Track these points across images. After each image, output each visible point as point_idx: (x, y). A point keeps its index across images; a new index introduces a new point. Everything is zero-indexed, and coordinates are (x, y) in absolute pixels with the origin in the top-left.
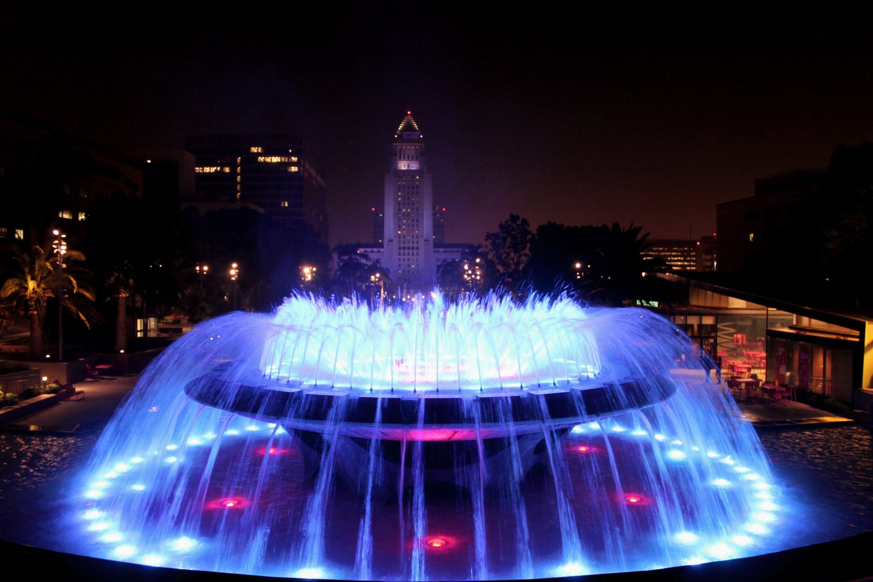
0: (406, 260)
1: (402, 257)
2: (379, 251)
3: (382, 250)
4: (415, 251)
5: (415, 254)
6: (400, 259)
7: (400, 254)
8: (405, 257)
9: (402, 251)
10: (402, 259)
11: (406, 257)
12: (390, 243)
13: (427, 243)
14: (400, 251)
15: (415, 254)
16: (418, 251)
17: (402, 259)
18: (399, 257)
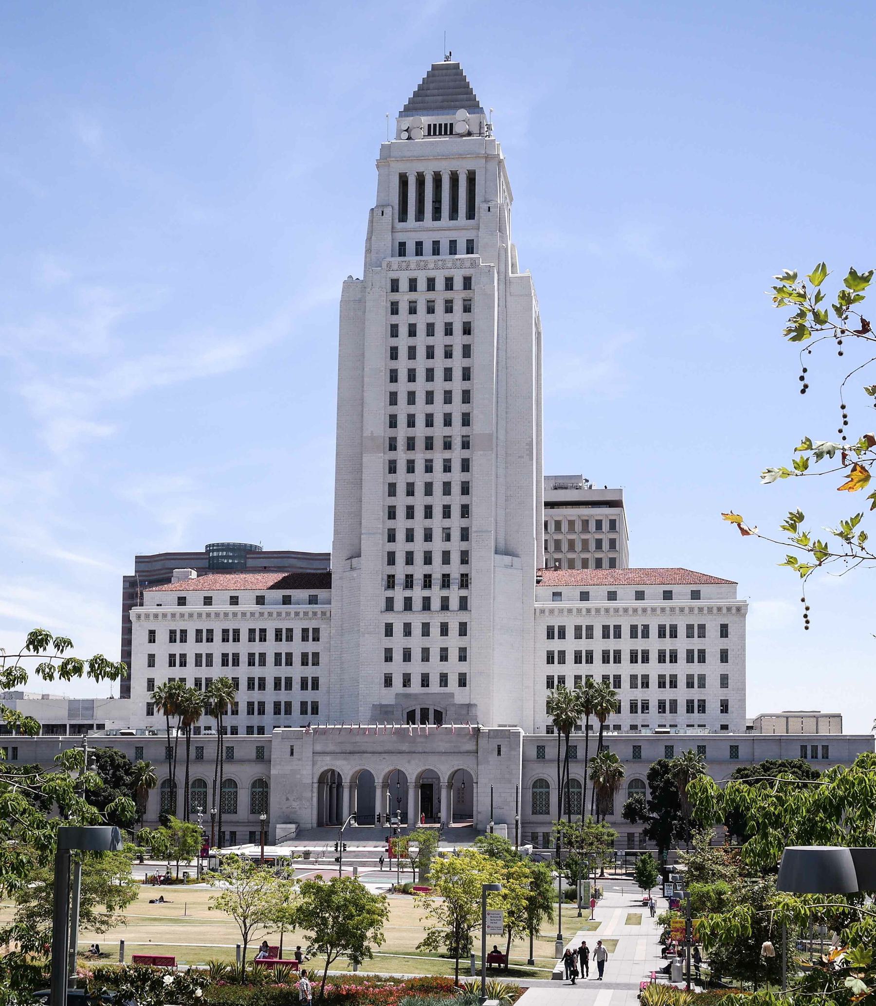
0: (417, 630)
1: (398, 621)
2: (313, 600)
3: (321, 593)
4: (454, 594)
5: (454, 604)
6: (389, 630)
7: (390, 605)
8: (408, 617)
9: (399, 594)
10: (398, 629)
11: (417, 620)
12: (354, 560)
13: (507, 559)
14: (389, 593)
15: (454, 604)
16: (464, 593)
17: (398, 629)
18: (390, 618)
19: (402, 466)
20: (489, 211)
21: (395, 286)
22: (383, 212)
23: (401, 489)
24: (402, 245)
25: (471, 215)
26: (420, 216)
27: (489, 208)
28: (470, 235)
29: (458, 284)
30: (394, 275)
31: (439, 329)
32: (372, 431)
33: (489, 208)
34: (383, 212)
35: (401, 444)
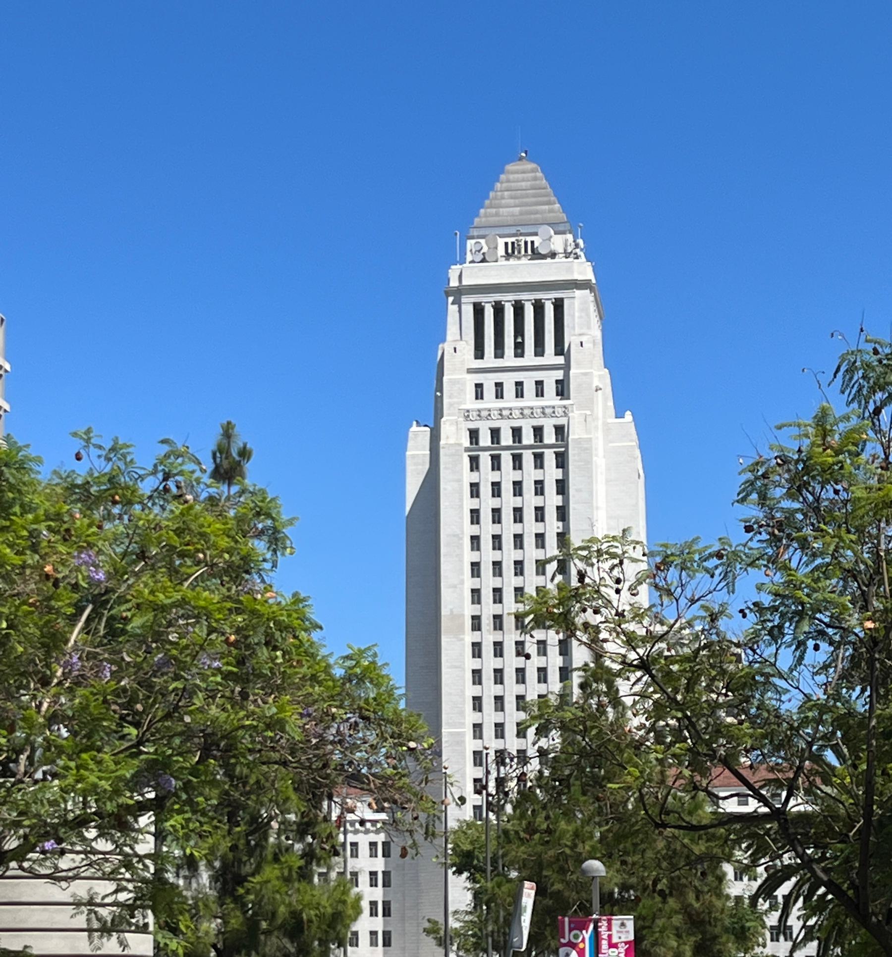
19: (488, 650)
20: (582, 345)
21: (474, 435)
22: (455, 349)
23: (488, 676)
24: (479, 387)
25: (560, 350)
26: (499, 352)
27: (582, 343)
28: (559, 375)
29: (550, 437)
30: (473, 426)
31: (529, 488)
32: (451, 610)
33: (582, 343)
34: (455, 349)
35: (487, 622)
